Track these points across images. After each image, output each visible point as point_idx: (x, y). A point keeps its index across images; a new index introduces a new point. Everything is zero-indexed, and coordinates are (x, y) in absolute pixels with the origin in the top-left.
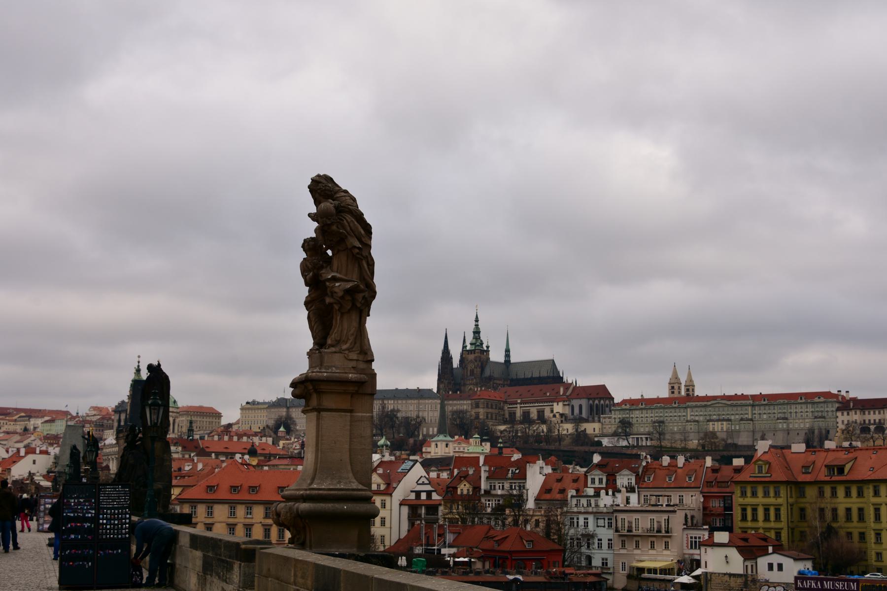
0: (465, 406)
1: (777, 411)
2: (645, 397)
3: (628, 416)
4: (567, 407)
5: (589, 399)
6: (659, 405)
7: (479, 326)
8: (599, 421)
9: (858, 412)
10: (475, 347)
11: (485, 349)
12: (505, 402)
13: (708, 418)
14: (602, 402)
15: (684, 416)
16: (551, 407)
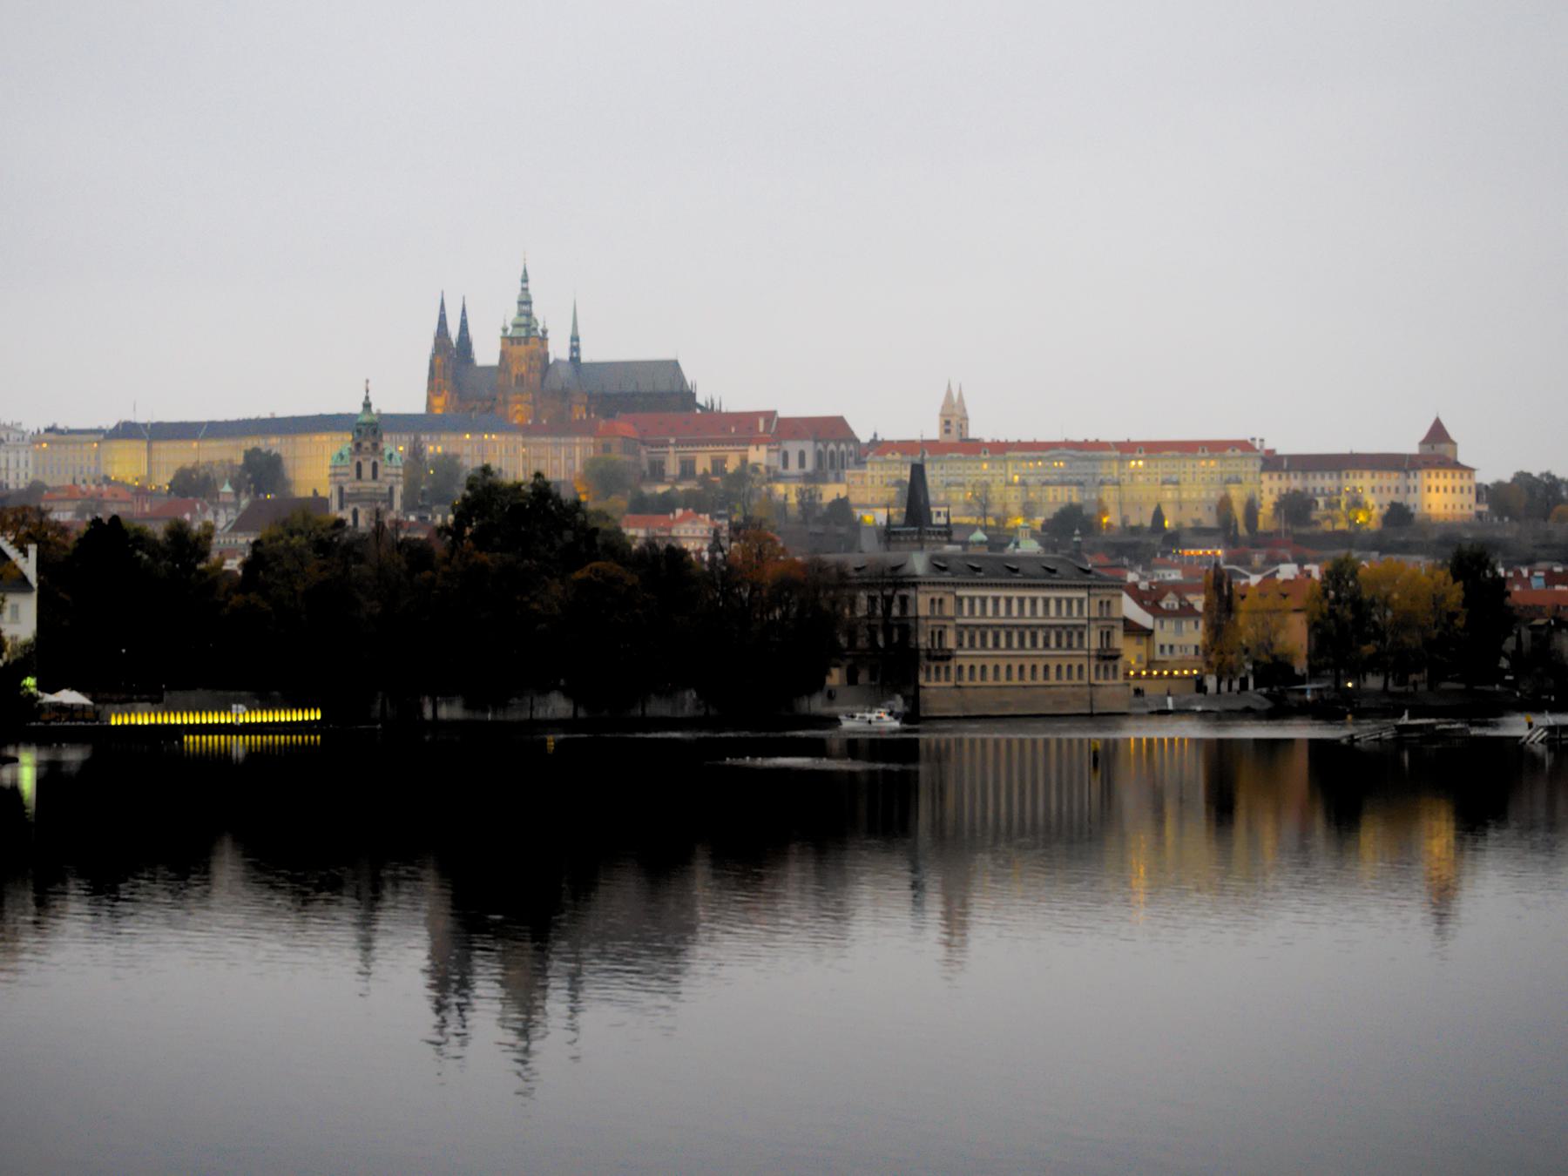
0: (563, 449)
1: (1162, 468)
2: (879, 438)
3: (897, 472)
4: (774, 455)
5: (816, 441)
6: (955, 455)
7: (531, 291)
8: (838, 480)
9: (1299, 475)
10: (528, 332)
11: (541, 334)
12: (644, 443)
13: (1044, 479)
14: (843, 447)
15: (1001, 475)
16: (745, 453)
